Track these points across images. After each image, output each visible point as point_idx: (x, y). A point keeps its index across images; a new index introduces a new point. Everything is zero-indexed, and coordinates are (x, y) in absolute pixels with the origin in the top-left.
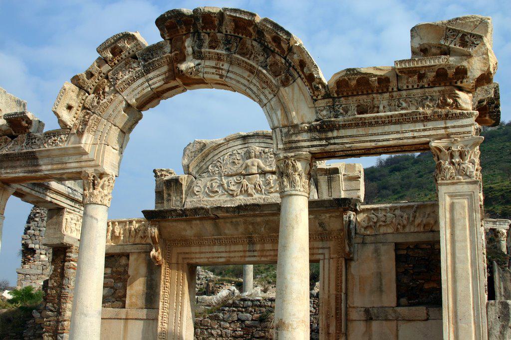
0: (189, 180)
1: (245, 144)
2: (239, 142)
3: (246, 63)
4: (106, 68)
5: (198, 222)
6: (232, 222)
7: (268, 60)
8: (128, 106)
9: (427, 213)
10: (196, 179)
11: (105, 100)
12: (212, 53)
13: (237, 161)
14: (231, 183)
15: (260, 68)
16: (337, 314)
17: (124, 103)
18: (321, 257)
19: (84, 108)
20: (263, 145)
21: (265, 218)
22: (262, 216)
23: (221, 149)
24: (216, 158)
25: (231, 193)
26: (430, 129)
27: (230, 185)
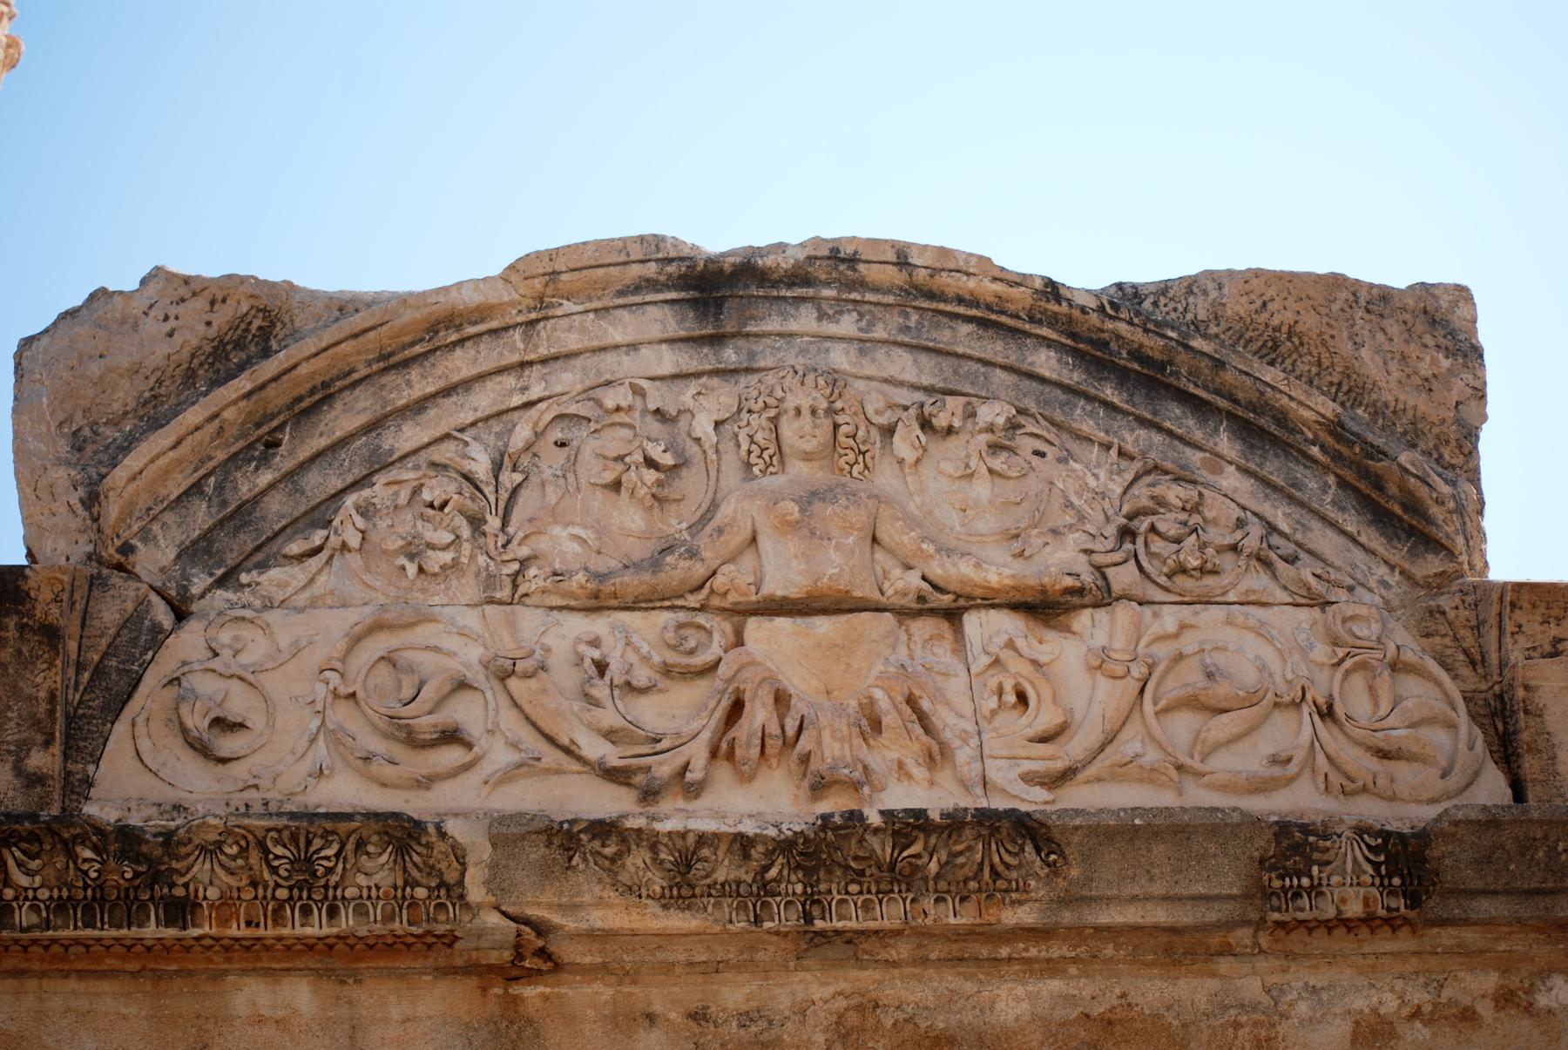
0: (110, 613)
1: (716, 340)
2: (657, 320)
5: (300, 995)
6: (699, 1016)
10: (181, 615)
13: (651, 476)
14: (601, 667)
20: (903, 365)
21: (1086, 988)
22: (1052, 968)
23: (461, 364)
24: (409, 435)
25: (612, 755)
27: (600, 690)
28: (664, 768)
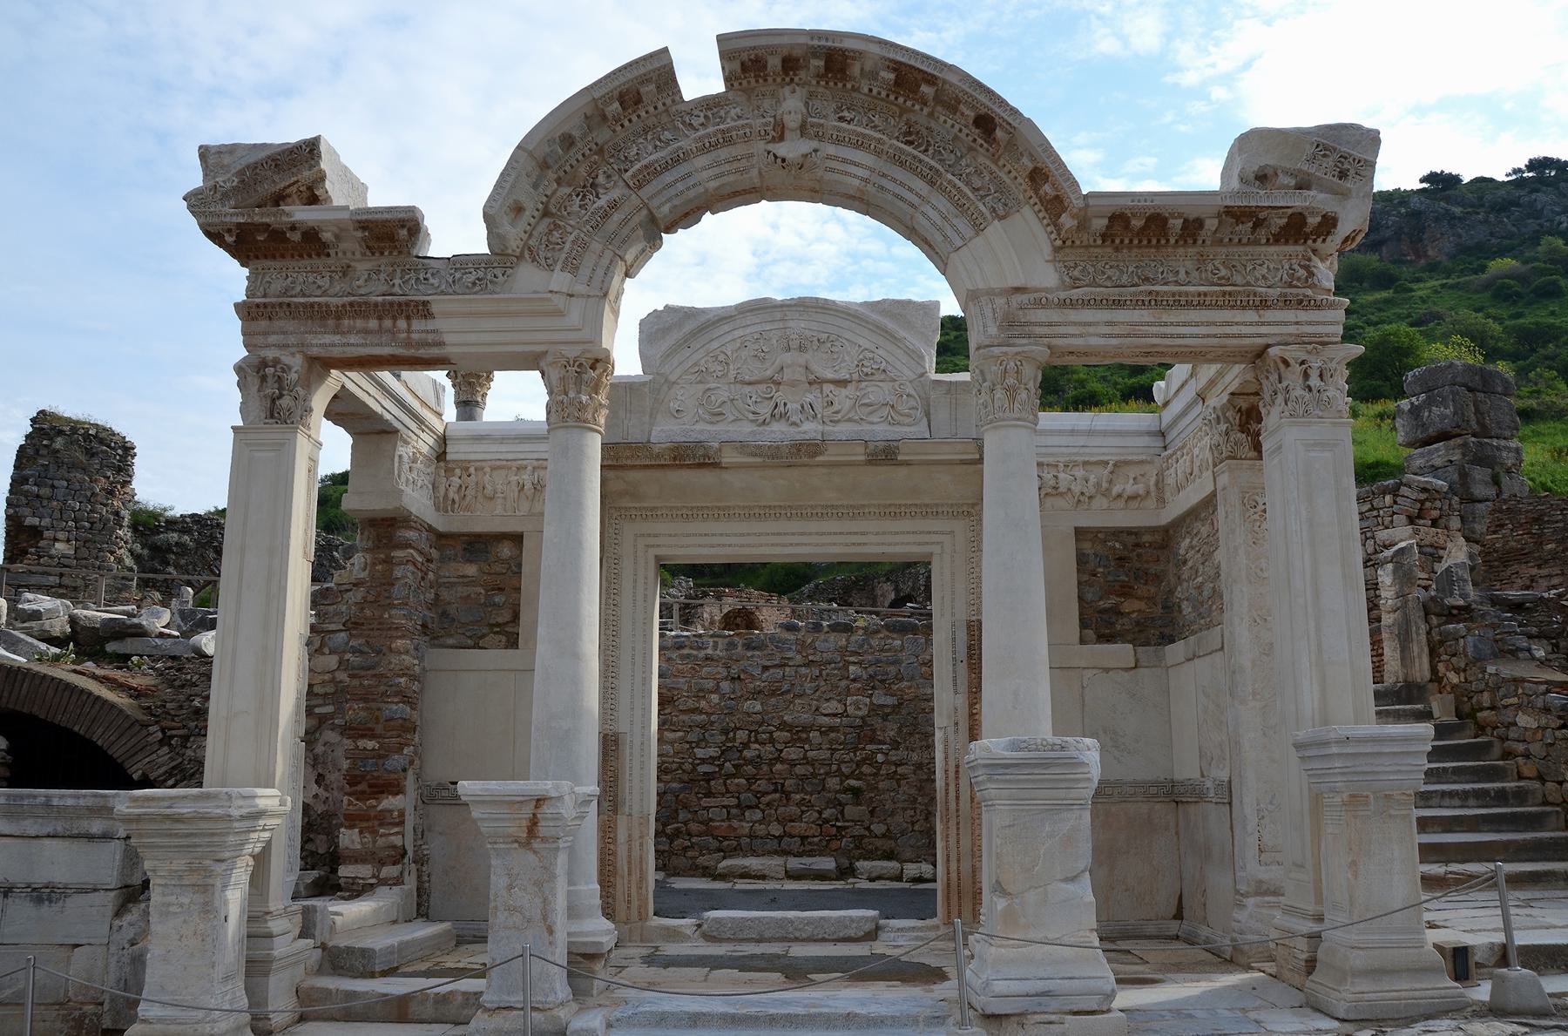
3: (920, 161)
4: (603, 135)
7: (963, 162)
8: (652, 219)
9: (1132, 475)
11: (602, 202)
12: (845, 130)
15: (950, 176)
16: (970, 657)
17: (645, 212)
18: (936, 549)
19: (546, 213)
23: (726, 328)
24: (715, 344)
26: (1269, 324)
28: (761, 419)
